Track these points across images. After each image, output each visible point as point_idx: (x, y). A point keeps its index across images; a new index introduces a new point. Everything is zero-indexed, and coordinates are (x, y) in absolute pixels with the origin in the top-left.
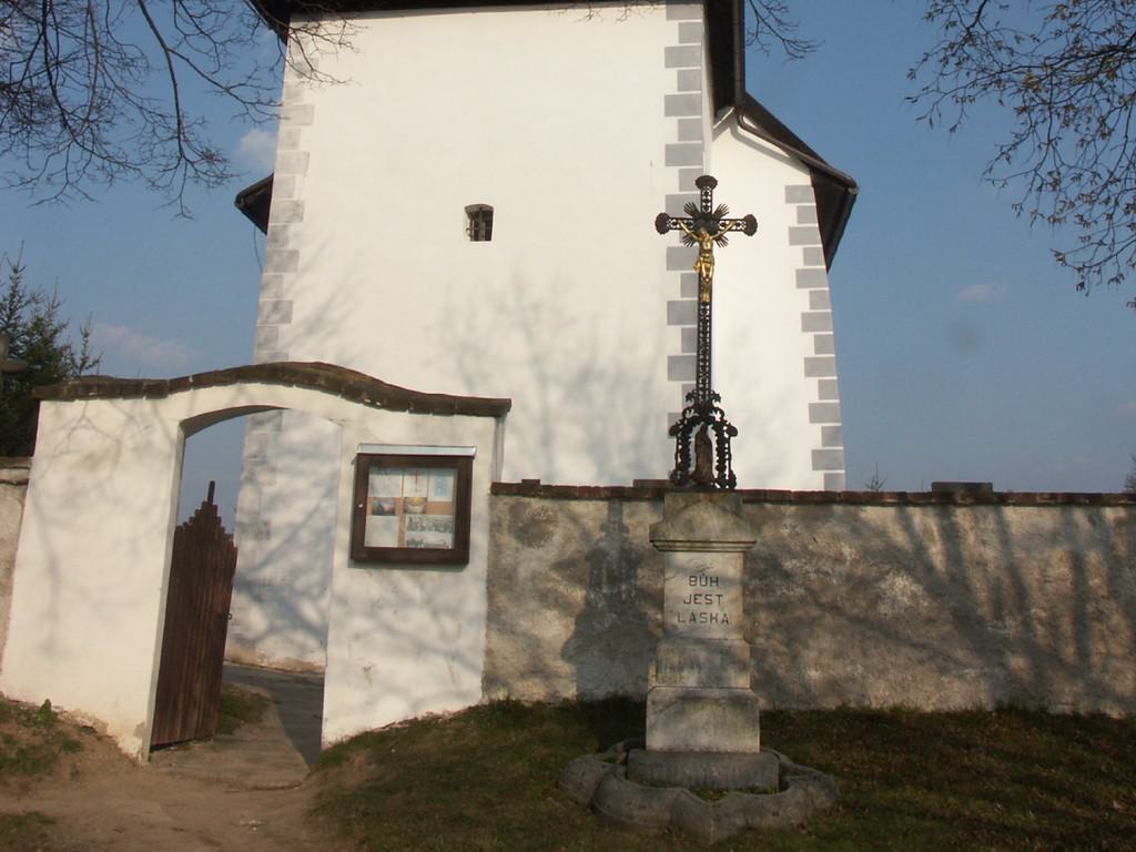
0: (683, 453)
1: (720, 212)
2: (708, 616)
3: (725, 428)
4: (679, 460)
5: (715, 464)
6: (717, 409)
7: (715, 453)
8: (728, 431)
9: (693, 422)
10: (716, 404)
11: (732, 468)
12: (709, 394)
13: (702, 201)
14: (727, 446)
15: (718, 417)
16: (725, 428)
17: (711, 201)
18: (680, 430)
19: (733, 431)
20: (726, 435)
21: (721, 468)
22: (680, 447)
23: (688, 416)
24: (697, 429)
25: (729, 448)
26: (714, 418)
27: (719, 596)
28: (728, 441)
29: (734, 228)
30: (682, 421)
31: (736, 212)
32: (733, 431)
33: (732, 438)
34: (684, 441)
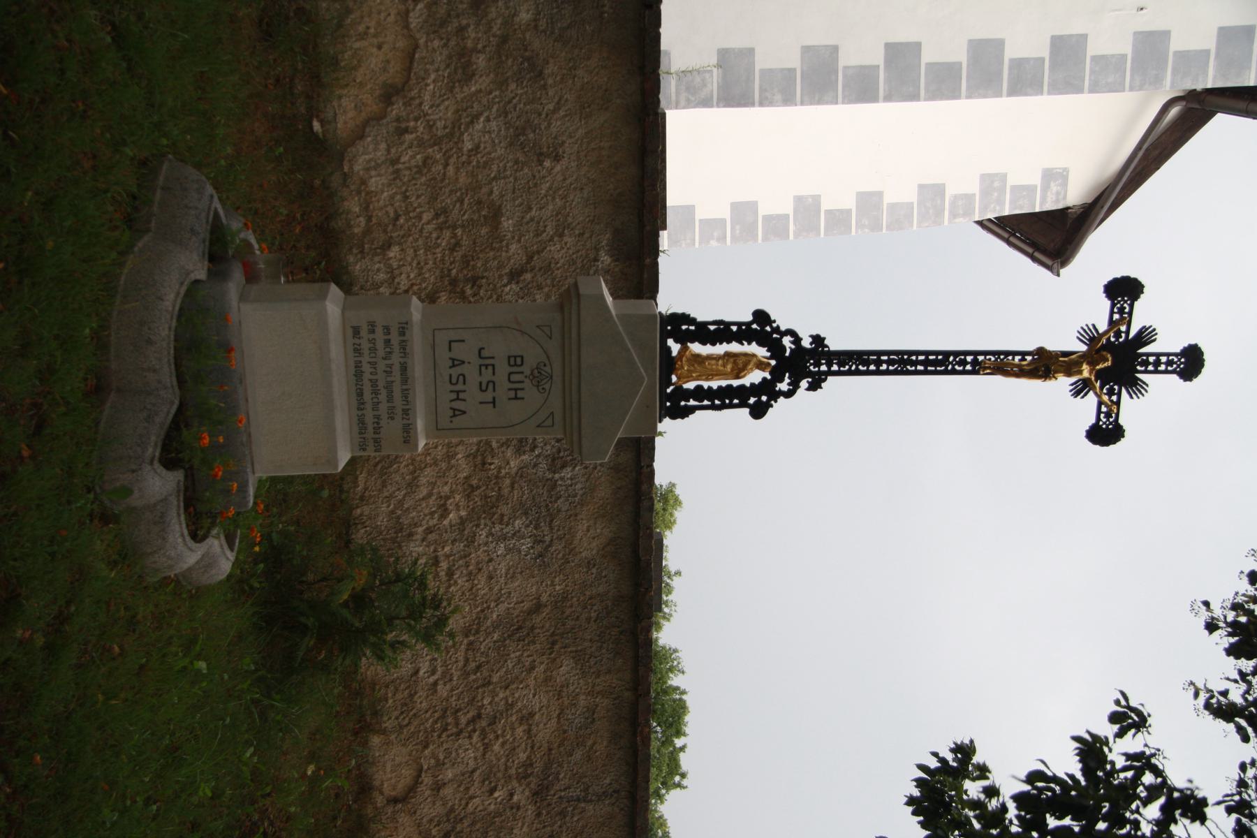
0: (723, 332)
1: (1145, 336)
2: (460, 387)
3: (764, 398)
4: (712, 328)
5: (706, 385)
6: (795, 386)
7: (724, 383)
8: (759, 402)
9: (776, 349)
10: (804, 384)
12: (820, 373)
13: (1158, 355)
14: (736, 401)
15: (783, 386)
16: (764, 398)
17: (1156, 372)
18: (760, 328)
19: (758, 412)
20: (752, 400)
21: (699, 393)
22: (734, 328)
23: (787, 341)
24: (761, 352)
25: (731, 406)
26: (782, 381)
27: (494, 402)
28: (743, 404)
29: (1104, 409)
30: (777, 330)
31: (1131, 410)
32: (758, 412)
33: (747, 410)
34: (744, 333)
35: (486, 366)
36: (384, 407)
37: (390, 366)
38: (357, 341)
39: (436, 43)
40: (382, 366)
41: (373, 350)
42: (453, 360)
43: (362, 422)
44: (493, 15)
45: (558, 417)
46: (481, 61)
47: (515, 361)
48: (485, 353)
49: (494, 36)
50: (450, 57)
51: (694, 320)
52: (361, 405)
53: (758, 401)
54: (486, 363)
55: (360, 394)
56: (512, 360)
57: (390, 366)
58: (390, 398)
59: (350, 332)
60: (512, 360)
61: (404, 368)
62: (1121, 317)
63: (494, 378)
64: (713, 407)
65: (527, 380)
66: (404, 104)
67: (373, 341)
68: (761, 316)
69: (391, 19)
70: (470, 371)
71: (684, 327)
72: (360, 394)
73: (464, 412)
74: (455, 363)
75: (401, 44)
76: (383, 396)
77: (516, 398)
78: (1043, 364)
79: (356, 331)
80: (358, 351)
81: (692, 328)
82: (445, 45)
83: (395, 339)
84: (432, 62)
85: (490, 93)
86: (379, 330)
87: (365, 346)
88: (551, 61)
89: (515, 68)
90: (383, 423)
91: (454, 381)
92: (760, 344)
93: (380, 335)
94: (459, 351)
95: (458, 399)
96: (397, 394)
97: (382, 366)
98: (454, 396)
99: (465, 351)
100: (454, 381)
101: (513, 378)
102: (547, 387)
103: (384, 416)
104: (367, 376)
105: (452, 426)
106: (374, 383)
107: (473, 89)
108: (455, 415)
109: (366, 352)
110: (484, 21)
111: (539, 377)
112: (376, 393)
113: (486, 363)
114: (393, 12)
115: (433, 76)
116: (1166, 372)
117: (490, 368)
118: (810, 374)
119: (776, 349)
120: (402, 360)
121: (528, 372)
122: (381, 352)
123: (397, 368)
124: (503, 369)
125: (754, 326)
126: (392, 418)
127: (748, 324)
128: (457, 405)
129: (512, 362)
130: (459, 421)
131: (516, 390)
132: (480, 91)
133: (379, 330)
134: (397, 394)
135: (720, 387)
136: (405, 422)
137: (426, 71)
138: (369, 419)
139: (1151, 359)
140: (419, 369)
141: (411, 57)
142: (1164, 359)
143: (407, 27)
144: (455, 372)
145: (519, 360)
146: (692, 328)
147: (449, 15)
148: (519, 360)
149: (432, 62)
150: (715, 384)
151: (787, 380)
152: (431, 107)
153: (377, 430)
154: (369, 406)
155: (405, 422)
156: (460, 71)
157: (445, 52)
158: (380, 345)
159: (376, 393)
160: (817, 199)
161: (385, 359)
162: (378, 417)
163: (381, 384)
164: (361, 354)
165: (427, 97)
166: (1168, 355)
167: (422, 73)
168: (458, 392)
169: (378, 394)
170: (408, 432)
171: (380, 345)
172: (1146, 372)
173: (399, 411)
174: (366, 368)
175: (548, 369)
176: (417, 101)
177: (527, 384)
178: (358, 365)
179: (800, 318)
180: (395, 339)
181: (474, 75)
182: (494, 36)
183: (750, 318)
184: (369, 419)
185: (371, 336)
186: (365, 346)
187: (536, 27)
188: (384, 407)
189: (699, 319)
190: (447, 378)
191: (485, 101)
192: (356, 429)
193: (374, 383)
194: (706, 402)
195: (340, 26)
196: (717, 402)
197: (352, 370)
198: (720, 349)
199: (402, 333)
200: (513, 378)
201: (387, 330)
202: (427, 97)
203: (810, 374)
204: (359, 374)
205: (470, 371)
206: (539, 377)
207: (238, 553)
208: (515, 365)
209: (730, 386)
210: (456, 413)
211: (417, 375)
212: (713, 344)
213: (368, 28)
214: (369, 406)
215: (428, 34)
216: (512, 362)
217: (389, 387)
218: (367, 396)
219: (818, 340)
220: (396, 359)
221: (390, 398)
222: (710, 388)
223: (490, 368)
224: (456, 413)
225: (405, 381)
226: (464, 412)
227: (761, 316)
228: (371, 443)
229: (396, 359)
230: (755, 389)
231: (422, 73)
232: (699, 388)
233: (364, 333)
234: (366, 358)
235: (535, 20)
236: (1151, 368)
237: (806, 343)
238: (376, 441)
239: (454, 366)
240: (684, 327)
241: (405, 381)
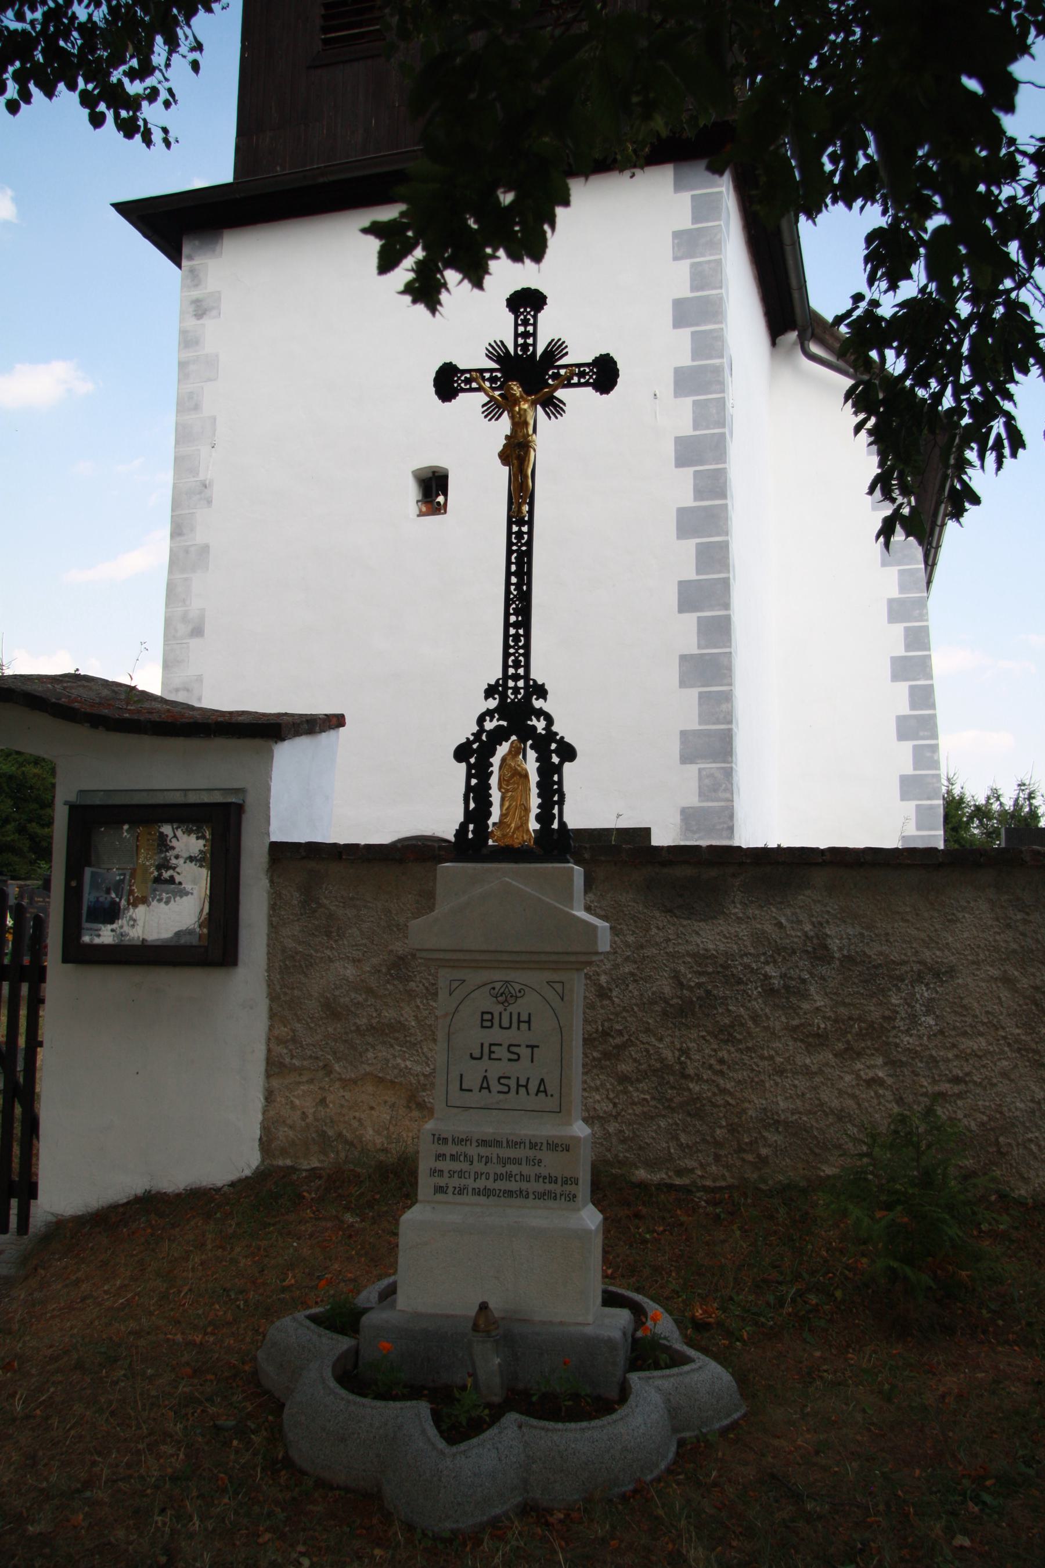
0: (477, 794)
1: (555, 351)
2: (512, 1083)
3: (553, 746)
4: (472, 805)
5: (535, 811)
6: (540, 713)
7: (534, 791)
8: (556, 751)
9: (498, 736)
10: (538, 704)
11: (565, 819)
12: (527, 686)
13: (517, 335)
14: (556, 778)
15: (540, 725)
16: (553, 746)
17: (534, 335)
18: (473, 754)
19: (568, 753)
20: (555, 759)
21: (545, 817)
22: (474, 782)
23: (489, 725)
24: (503, 749)
25: (560, 782)
26: (534, 728)
27: (532, 1047)
28: (558, 769)
29: (575, 380)
30: (477, 736)
31: (580, 352)
32: (568, 753)
33: (567, 766)
34: (479, 772)
35: (491, 1052)
36: (526, 1170)
37: (480, 1157)
38: (450, 1190)
39: (370, 1055)
40: (479, 1167)
41: (461, 1174)
42: (482, 1088)
43: (541, 1196)
44: (346, 1000)
45: (555, 977)
46: (389, 1014)
47: (486, 1020)
48: (477, 1053)
49: (366, 1000)
50: (384, 1043)
51: (461, 825)
52: (523, 1194)
53: (555, 753)
54: (486, 1052)
55: (510, 1193)
56: (486, 1024)
57: (480, 1157)
58: (518, 1162)
59: (440, 1197)
60: (486, 1024)
61: (484, 1143)
62: (473, 379)
63: (505, 1046)
64: (561, 802)
65: (510, 1009)
66: (424, 1090)
67: (452, 1174)
68: (462, 753)
69: (348, 1095)
70: (495, 1069)
71: (470, 836)
72: (510, 1193)
73: (542, 1080)
74: (485, 1085)
75: (370, 1089)
76: (514, 1169)
77: (529, 1022)
78: (517, 453)
79: (440, 1190)
80: (461, 1191)
81: (471, 827)
82: (373, 1047)
83: (450, 1149)
84: (387, 1060)
85: (418, 1007)
86: (440, 1165)
87: (456, 1182)
88: (390, 948)
89: (396, 982)
90: (544, 1172)
91: (506, 1089)
92: (493, 753)
93: (446, 1165)
94: (473, 1080)
95: (526, 1087)
96: (511, 1153)
97: (479, 1167)
98: (522, 1090)
99: (473, 1075)
100: (506, 1089)
101: (505, 1023)
102: (517, 987)
103: (537, 1170)
104: (490, 1184)
105: (557, 1096)
106: (498, 1177)
107: (413, 1023)
108: (545, 1092)
109: (463, 1182)
110: (353, 1009)
111: (506, 996)
112: (510, 1176)
113: (486, 1052)
114: (341, 1093)
115: (399, 1060)
116: (535, 325)
117: (493, 1048)
118: (528, 697)
119: (498, 736)
120: (474, 1144)
121: (500, 1008)
122: (464, 1166)
123: (484, 1151)
124: (495, 1034)
125: (472, 760)
126: (540, 1161)
127: (470, 767)
128: (533, 1087)
129: (489, 1024)
130: (552, 1086)
131: (519, 1022)
132: (416, 1017)
133: (440, 1165)
134: (511, 1153)
135: (539, 796)
136: (544, 1147)
137: (394, 1067)
138: (540, 1187)
139: (520, 341)
140: (487, 1127)
141: (381, 1080)
142: (521, 329)
143: (355, 1082)
144: (495, 1087)
145: (487, 1017)
146: (471, 827)
147: (346, 1041)
148: (487, 1017)
149: (387, 1060)
150: (535, 801)
151: (534, 722)
152: (428, 1066)
153: (553, 1180)
154: (524, 1186)
155: (544, 1147)
156: (397, 1035)
157: (379, 1047)
158: (456, 1166)
159: (510, 1176)
160: (895, 660)
161: (472, 1163)
162: (538, 1177)
163: (500, 1170)
164: (466, 1188)
165: (418, 1068)
166: (516, 325)
167: (396, 1071)
168: (518, 1086)
169: (515, 1175)
170: (557, 1145)
171: (456, 1166)
172: (534, 345)
173: (531, 1153)
174: (481, 1184)
175: (498, 985)
176: (422, 1078)
177: (513, 1009)
178: (477, 1192)
179: (464, 713)
180: (450, 1149)
181: (400, 1022)
182: (366, 1000)
183: (464, 765)
184: (540, 1187)
185: (446, 1174)
186: (456, 1182)
187: (359, 961)
188: (526, 1170)
189: (462, 819)
190: (502, 1096)
191: (425, 1013)
192: (550, 1203)
193: (498, 1177)
194: (556, 811)
195: (352, 1144)
196: (556, 798)
197: (482, 1199)
198: (496, 795)
199: (445, 1140)
200: (505, 1023)
201: (440, 1157)
202: (418, 1068)
203: (528, 697)
204: (487, 1193)
205: (495, 1069)
206: (506, 996)
207: (705, 1351)
208: (491, 1020)
209: (539, 785)
210: (542, 1089)
211: (491, 1130)
212: (490, 804)
213: (355, 1118)
214: (524, 1186)
215: (362, 1062)
216: (489, 1024)
217: (504, 1162)
218: (513, 1186)
219: (490, 692)
220: (472, 1150)
221: (518, 1162)
222: (539, 807)
223: (493, 1048)
224: (542, 1089)
225: (498, 1143)
226: (542, 1080)
227: (462, 753)
228: (568, 1188)
229: (472, 1150)
230: (543, 759)
231: (396, 1071)
232: (538, 818)
233: (442, 1182)
234: (470, 1183)
235: (354, 961)
236: (530, 341)
237: (493, 703)
238: (565, 1182)
239: (488, 1088)
240: (470, 836)
241: (498, 1143)
